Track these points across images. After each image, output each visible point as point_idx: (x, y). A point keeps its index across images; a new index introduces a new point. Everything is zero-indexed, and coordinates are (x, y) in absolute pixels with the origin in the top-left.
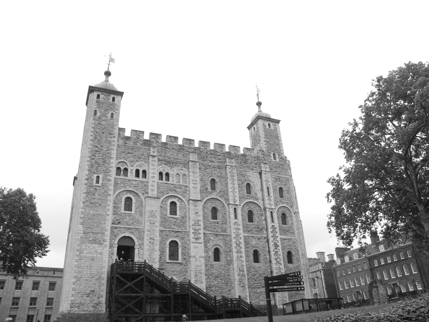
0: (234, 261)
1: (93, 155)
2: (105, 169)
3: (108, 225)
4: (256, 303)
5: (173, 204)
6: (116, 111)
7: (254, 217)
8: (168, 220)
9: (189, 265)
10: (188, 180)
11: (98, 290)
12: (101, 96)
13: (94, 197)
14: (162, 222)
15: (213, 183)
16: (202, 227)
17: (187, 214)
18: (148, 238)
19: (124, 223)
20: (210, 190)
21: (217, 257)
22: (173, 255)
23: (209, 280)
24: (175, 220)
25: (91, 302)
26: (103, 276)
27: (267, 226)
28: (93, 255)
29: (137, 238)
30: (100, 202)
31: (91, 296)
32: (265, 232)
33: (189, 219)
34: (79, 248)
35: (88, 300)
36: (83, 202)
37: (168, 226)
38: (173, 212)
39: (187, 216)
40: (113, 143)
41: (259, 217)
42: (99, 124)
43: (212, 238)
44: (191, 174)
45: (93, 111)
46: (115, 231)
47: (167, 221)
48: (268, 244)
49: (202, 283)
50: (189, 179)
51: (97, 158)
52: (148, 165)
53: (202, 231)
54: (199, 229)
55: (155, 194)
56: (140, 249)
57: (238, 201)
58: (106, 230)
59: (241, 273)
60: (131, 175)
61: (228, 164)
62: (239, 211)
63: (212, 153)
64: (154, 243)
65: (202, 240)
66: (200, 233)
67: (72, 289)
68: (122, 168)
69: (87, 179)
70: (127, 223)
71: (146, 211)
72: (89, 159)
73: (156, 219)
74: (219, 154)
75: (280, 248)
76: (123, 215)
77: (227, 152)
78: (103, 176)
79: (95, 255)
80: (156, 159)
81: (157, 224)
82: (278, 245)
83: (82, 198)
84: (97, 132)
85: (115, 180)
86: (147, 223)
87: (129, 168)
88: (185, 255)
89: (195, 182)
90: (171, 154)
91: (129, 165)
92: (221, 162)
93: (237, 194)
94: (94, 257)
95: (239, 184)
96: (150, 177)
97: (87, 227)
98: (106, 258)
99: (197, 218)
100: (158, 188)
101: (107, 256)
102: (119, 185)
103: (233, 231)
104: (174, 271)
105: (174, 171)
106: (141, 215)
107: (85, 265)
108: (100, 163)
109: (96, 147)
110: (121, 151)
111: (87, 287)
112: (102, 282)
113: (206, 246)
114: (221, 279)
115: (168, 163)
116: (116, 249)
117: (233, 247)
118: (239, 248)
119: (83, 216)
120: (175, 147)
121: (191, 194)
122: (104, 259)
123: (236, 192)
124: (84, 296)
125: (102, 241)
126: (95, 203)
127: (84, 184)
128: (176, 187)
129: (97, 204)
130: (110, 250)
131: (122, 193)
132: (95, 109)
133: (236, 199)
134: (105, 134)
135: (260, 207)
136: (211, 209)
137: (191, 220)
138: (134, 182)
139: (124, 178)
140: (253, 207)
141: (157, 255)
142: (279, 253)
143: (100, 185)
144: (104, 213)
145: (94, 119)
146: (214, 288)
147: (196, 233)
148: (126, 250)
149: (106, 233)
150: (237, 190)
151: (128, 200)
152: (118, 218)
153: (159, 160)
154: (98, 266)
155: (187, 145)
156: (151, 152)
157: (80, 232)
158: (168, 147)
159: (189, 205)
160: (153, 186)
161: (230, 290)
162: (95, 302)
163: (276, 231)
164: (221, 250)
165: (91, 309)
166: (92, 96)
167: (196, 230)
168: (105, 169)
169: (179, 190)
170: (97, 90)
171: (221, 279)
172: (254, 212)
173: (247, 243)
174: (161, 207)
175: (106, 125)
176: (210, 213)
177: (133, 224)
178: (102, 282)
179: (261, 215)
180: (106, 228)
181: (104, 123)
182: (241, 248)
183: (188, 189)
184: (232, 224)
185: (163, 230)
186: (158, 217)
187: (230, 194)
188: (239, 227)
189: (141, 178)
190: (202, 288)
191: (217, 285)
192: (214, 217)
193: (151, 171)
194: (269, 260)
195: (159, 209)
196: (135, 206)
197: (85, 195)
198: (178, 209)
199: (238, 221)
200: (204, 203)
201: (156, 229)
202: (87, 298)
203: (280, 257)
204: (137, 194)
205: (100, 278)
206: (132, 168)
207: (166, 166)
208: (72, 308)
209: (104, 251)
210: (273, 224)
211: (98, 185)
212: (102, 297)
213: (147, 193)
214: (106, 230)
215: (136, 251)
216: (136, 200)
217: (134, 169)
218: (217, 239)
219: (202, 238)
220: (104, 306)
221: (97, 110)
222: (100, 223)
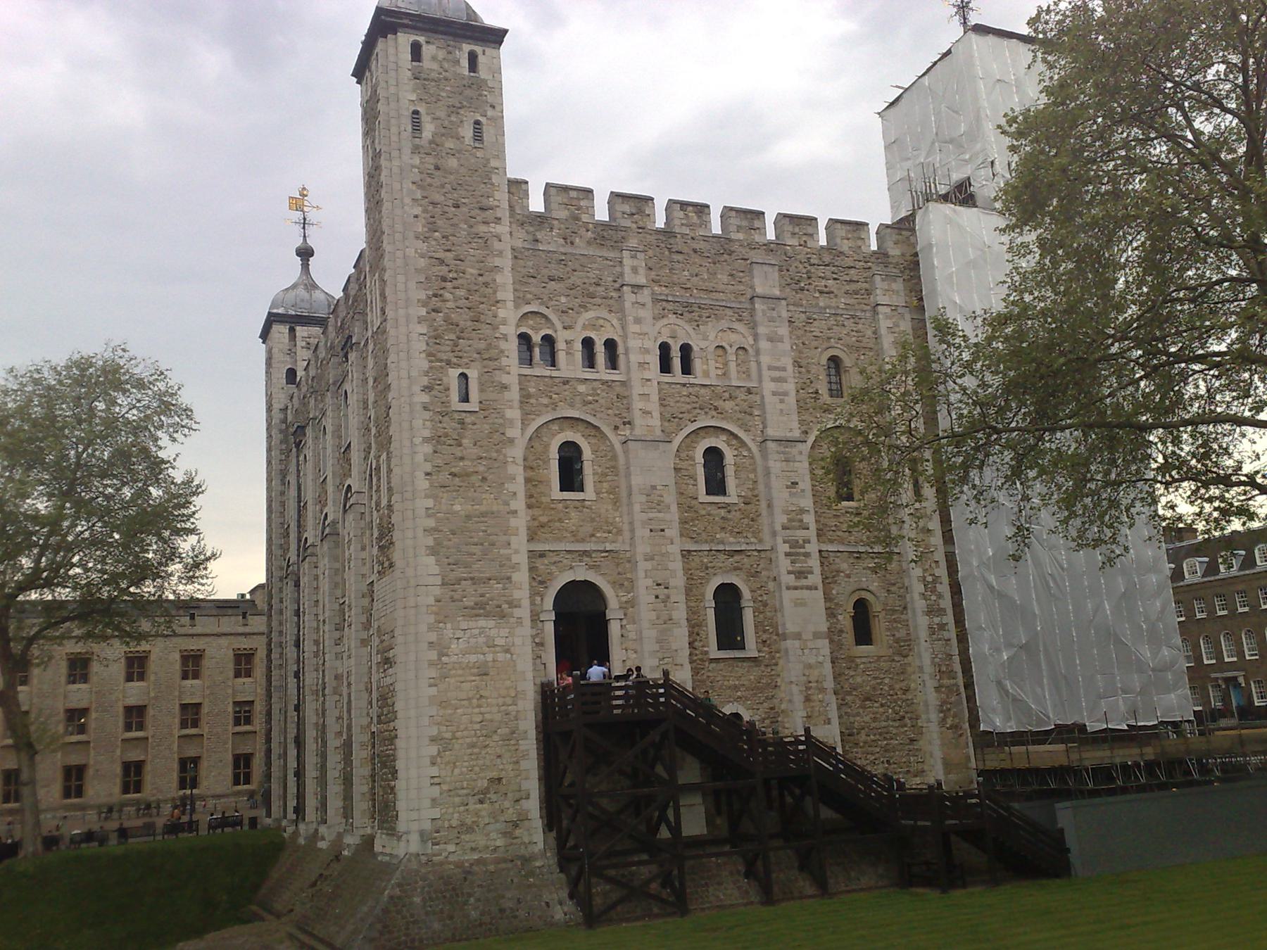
0: (922, 641)
1: (435, 295)
2: (482, 345)
3: (520, 547)
5: (713, 455)
6: (490, 113)
8: (703, 512)
9: (781, 662)
10: (753, 365)
11: (512, 774)
12: (428, 51)
13: (458, 452)
14: (684, 522)
15: (833, 371)
17: (761, 487)
18: (649, 582)
20: (825, 397)
22: (730, 634)
23: (845, 709)
24: (723, 512)
25: (493, 815)
29: (613, 583)
30: (481, 469)
31: (494, 797)
33: (769, 506)
34: (433, 637)
35: (484, 813)
36: (427, 474)
38: (716, 485)
39: (762, 497)
40: (497, 245)
42: (437, 168)
43: (844, 566)
44: (764, 345)
45: (408, 113)
46: (540, 563)
49: (828, 722)
50: (759, 363)
51: (450, 305)
52: (623, 320)
53: (813, 548)
55: (656, 422)
56: (624, 622)
58: (515, 567)
59: (946, 682)
60: (570, 364)
61: (881, 299)
63: (827, 259)
64: (668, 597)
65: (815, 578)
66: (807, 555)
67: (428, 781)
68: (536, 338)
69: (427, 389)
70: (574, 534)
71: (635, 490)
72: (423, 312)
74: (849, 262)
77: (874, 252)
78: (481, 375)
79: (490, 657)
80: (645, 296)
81: (673, 532)
83: (420, 458)
84: (434, 204)
85: (520, 384)
86: (642, 533)
87: (561, 337)
88: (765, 631)
89: (777, 374)
91: (559, 326)
96: (634, 366)
97: (450, 560)
98: (525, 664)
99: (794, 500)
100: (662, 400)
102: (532, 401)
104: (736, 688)
105: (706, 338)
106: (616, 502)
107: (463, 695)
108: (462, 323)
109: (442, 262)
110: (524, 271)
111: (477, 769)
113: (828, 598)
114: (882, 705)
115: (686, 310)
116: (550, 628)
117: (916, 596)
118: (933, 598)
119: (431, 523)
120: (701, 245)
121: (768, 416)
122: (520, 667)
124: (471, 800)
125: (505, 606)
126: (468, 475)
127: (419, 408)
129: (474, 478)
132: (412, 108)
134: (464, 209)
137: (777, 510)
138: (582, 388)
139: (548, 373)
141: (680, 637)
143: (473, 405)
144: (501, 508)
145: (416, 150)
146: (863, 737)
147: (798, 554)
148: (580, 624)
149: (516, 577)
152: (544, 519)
153: (656, 301)
154: (503, 692)
155: (741, 236)
156: (627, 270)
157: (431, 580)
158: (679, 248)
160: (645, 396)
161: (912, 740)
164: (876, 607)
165: (498, 843)
166: (391, 51)
167: (794, 544)
168: (482, 345)
169: (729, 405)
170: (407, 26)
171: (882, 705)
174: (677, 470)
175: (462, 170)
177: (593, 535)
180: (515, 559)
181: (453, 163)
182: (940, 596)
183: (758, 398)
185: (689, 551)
186: (674, 508)
189: (602, 371)
190: (831, 742)
191: (873, 725)
193: (634, 343)
195: (670, 479)
197: (428, 449)
198: (730, 471)
201: (671, 548)
202: (479, 806)
205: (513, 733)
206: (567, 335)
208: (437, 844)
209: (518, 641)
211: (465, 407)
212: (528, 798)
213: (629, 423)
214: (515, 567)
215: (614, 629)
216: (594, 452)
217: (578, 336)
219: (817, 570)
220: (536, 822)
221: (422, 109)
222: (493, 544)
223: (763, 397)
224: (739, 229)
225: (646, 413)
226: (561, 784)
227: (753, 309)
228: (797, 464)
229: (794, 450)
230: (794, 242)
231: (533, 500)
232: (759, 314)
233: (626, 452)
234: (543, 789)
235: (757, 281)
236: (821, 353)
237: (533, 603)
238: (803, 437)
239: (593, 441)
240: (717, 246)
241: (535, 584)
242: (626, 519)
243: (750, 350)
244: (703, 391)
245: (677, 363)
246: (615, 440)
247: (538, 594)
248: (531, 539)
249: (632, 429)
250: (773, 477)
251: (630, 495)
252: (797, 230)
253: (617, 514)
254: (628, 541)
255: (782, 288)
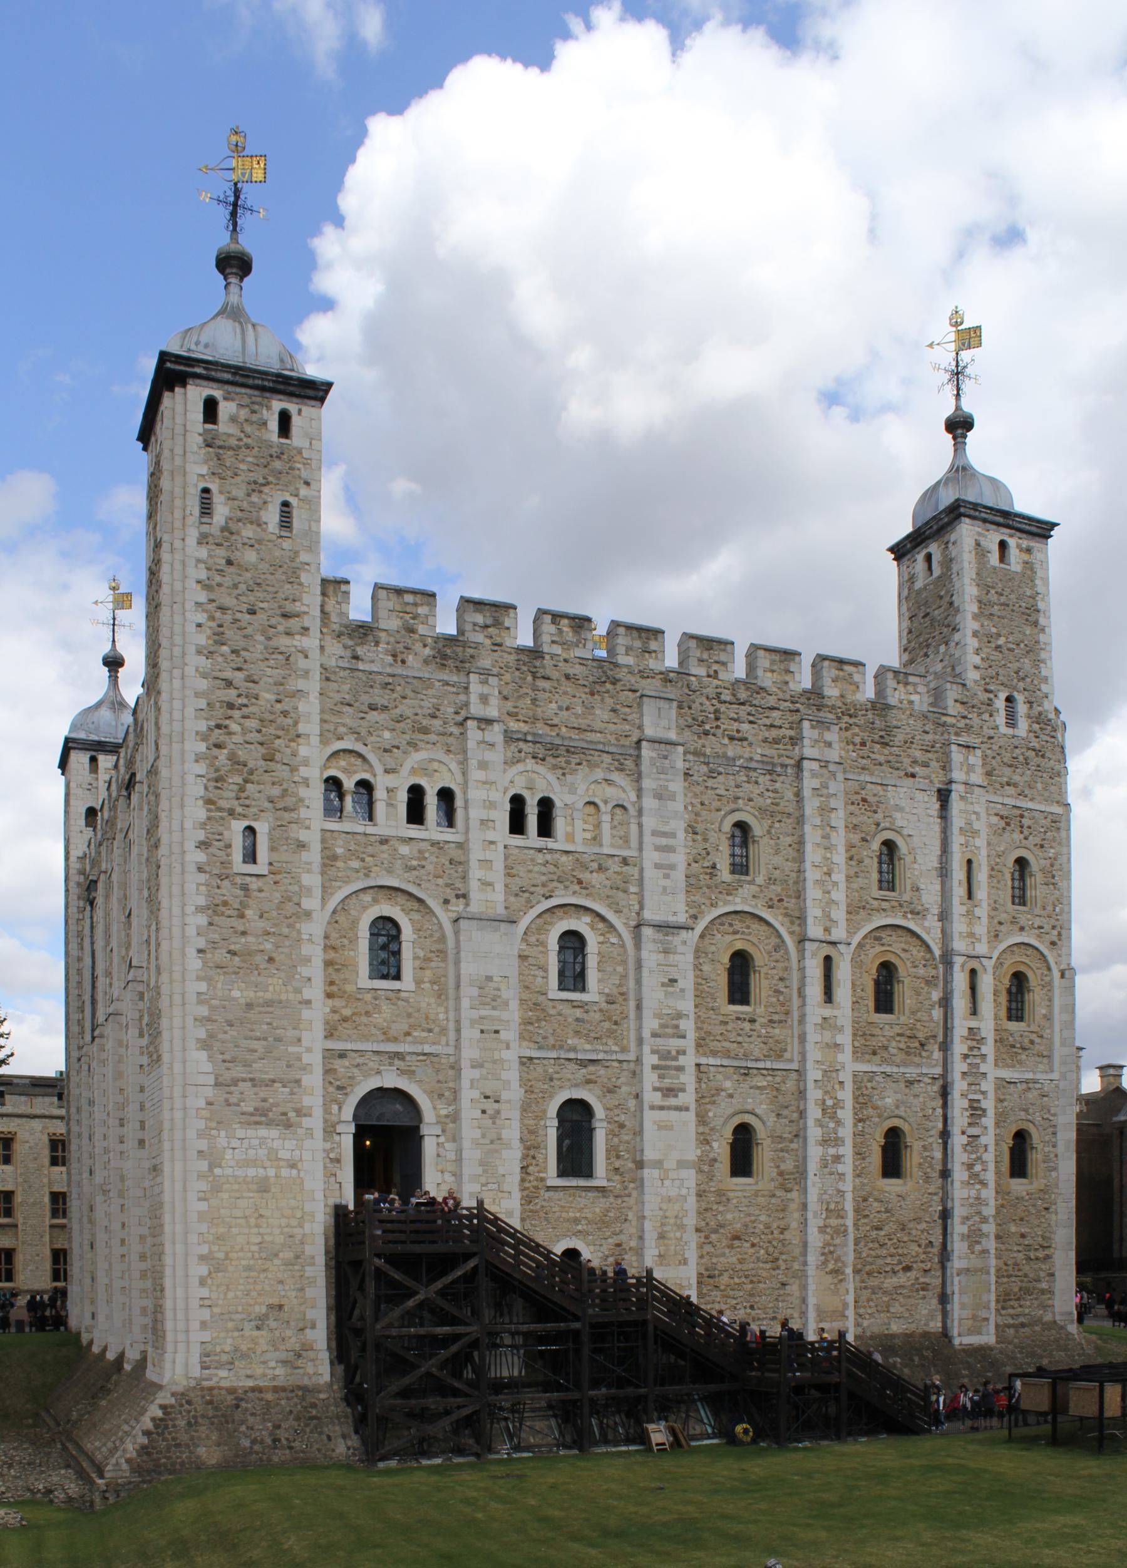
3: (312, 1044)
4: (876, 1330)
5: (573, 942)
7: (898, 989)
8: (552, 1012)
10: (634, 828)
11: (295, 1301)
14: (526, 1022)
16: (689, 1043)
19: (374, 1031)
20: (725, 874)
21: (742, 1160)
24: (578, 1013)
26: (309, 1250)
27: (947, 1029)
28: (261, 1171)
29: (429, 1093)
32: (937, 1055)
33: (639, 1007)
37: (551, 1041)
38: (573, 977)
39: (632, 996)
41: (918, 994)
44: (648, 802)
47: (547, 1017)
48: (945, 1105)
50: (640, 825)
54: (678, 1052)
55: (498, 896)
57: (843, 924)
62: (843, 972)
63: (743, 695)
73: (504, 1015)
74: (771, 701)
75: (989, 1121)
76: (368, 997)
79: (271, 1172)
82: (984, 1111)
89: (664, 841)
90: (563, 708)
92: (776, 741)
93: (840, 895)
94: (267, 1178)
95: (850, 847)
101: (320, 1174)
103: (814, 1054)
105: (573, 790)
106: (441, 995)
112: (307, 1275)
121: (647, 895)
122: (307, 1186)
123: (836, 884)
125: (292, 1114)
128: (584, 867)
130: (328, 1146)
131: (354, 900)
133: (833, 916)
135: (928, 948)
136: (726, 959)
140: (897, 947)
142: (983, 1140)
148: (386, 1143)
149: (306, 1080)
150: (839, 877)
151: (386, 934)
152: (347, 1012)
155: (630, 660)
159: (638, 946)
160: (486, 863)
162: (288, 1346)
163: (984, 1050)
169: (596, 879)
172: (902, 972)
173: (862, 1100)
174: (523, 958)
176: (723, 980)
177: (408, 1034)
178: (309, 1271)
179: (928, 983)
180: (306, 1059)
183: (635, 871)
184: (810, 1028)
186: (514, 1005)
187: (813, 893)
188: (839, 1039)
192: (739, 992)
194: (939, 1167)
195: (513, 972)
196: (416, 958)
198: (592, 962)
199: (836, 1012)
200: (702, 936)
203: (985, 1157)
204: (420, 901)
207: (540, 768)
209: (307, 1156)
210: (973, 1024)
212: (313, 1327)
213: (464, 896)
216: (417, 931)
218: (745, 1086)
223: (641, 870)
224: (629, 650)
225: (486, 884)
226: (350, 1317)
227: (639, 756)
228: (677, 957)
229: (677, 939)
230: (702, 671)
231: (334, 988)
232: (645, 766)
233: (457, 933)
234: (333, 1318)
235: (647, 721)
236: (725, 816)
237: (327, 1111)
238: (690, 922)
239: (416, 916)
240: (597, 673)
241: (331, 1089)
242: (451, 1015)
243: (632, 811)
244: (564, 858)
245: (532, 821)
246: (444, 917)
247: (335, 1101)
248: (329, 1035)
249: (467, 905)
250: (645, 972)
251: (458, 986)
252: (705, 656)
253: (442, 1009)
254: (452, 1043)
255: (681, 729)
